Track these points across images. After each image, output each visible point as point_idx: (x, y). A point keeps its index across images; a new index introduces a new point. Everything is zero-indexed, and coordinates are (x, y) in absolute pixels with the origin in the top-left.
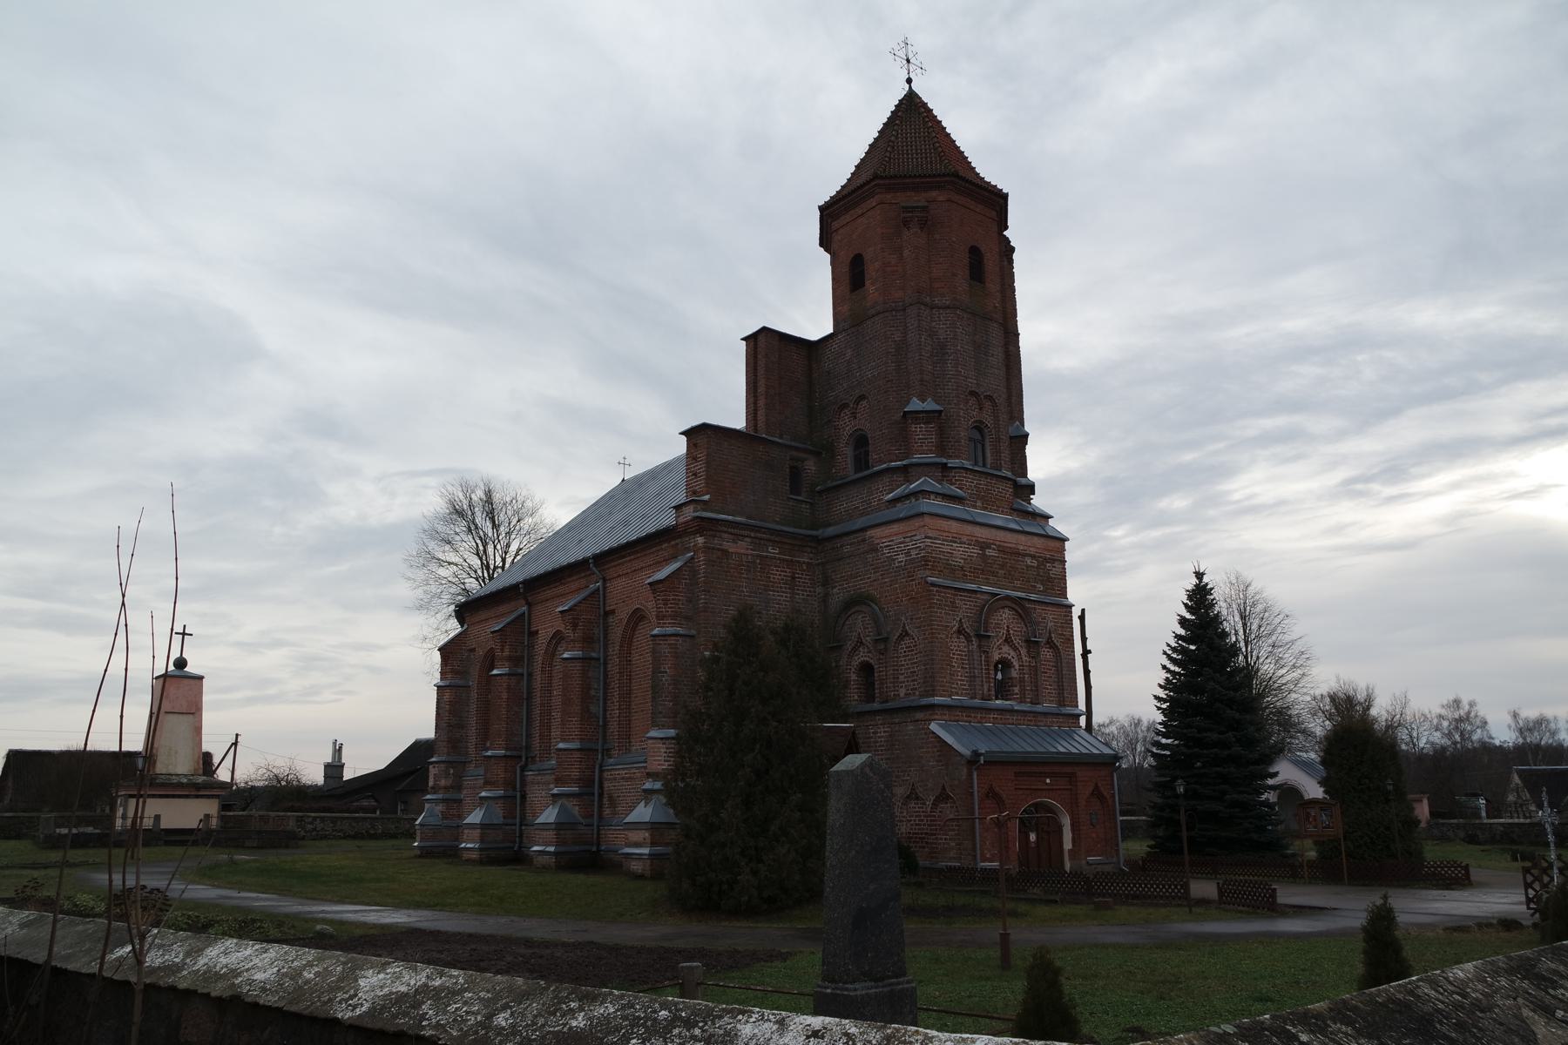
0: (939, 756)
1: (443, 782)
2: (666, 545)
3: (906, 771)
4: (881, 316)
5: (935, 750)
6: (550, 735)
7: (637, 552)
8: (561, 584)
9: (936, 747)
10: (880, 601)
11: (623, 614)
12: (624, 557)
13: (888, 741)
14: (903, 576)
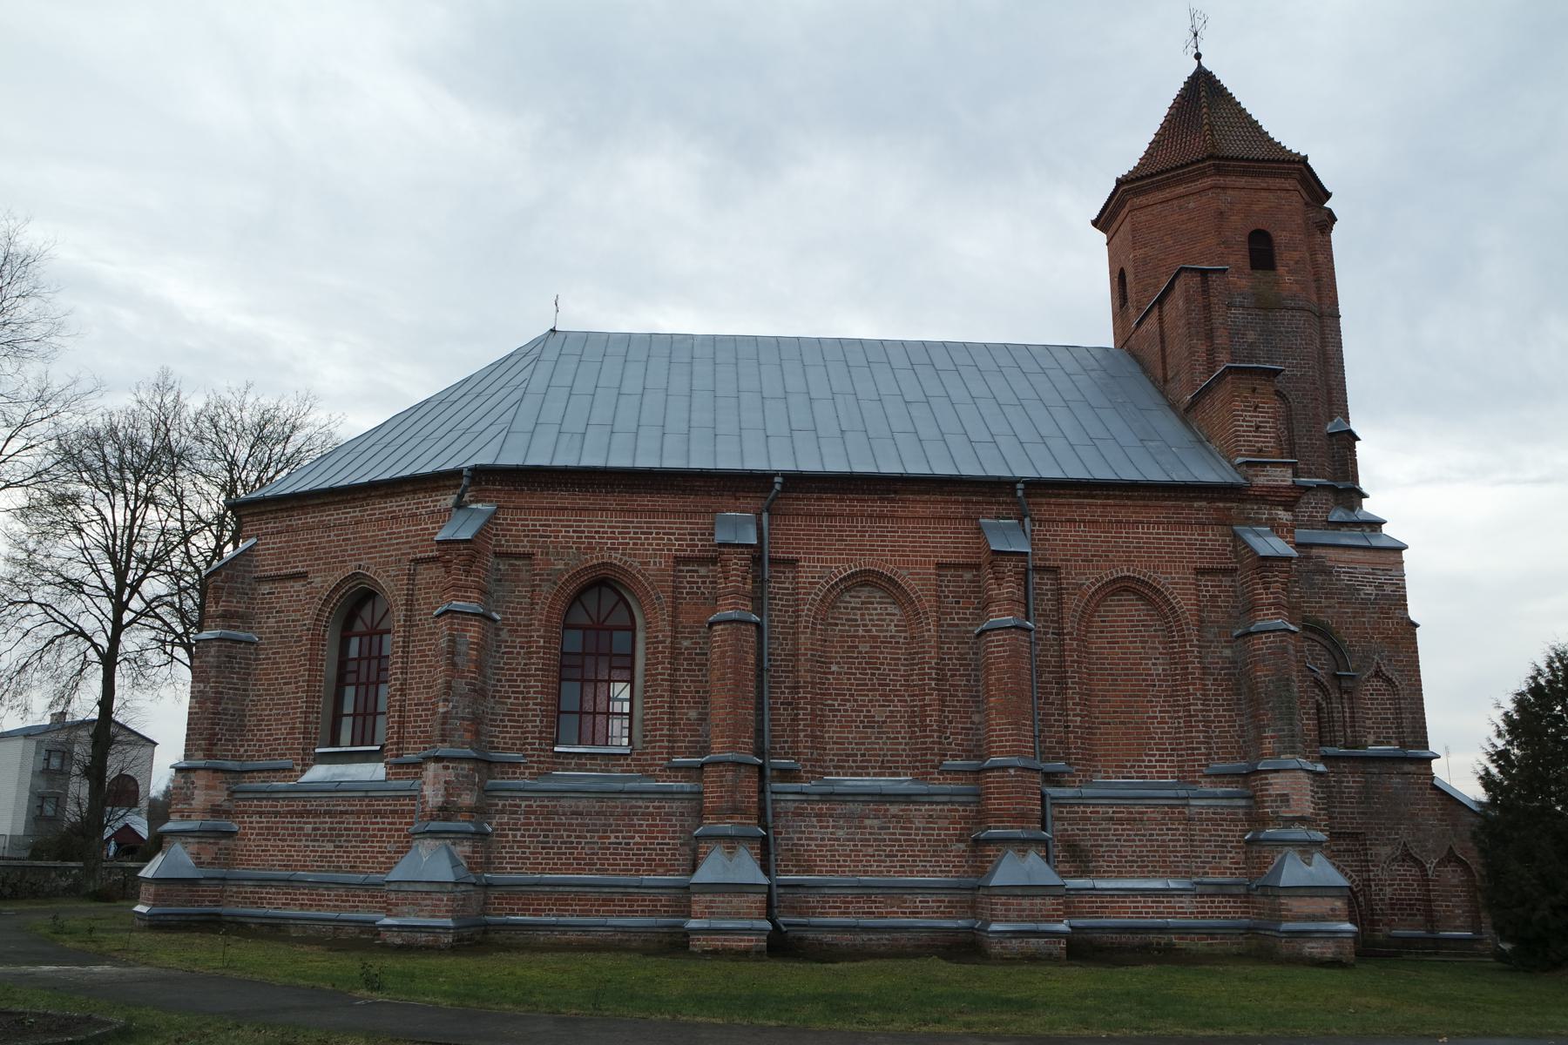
0: (1442, 815)
1: (467, 799)
2: (1204, 504)
3: (1392, 829)
4: (1306, 314)
5: (1437, 808)
6: (823, 737)
7: (1128, 498)
8: (882, 499)
9: (1437, 804)
10: (1338, 632)
11: (1091, 579)
12: (1093, 497)
13: (1360, 793)
14: (1371, 610)
